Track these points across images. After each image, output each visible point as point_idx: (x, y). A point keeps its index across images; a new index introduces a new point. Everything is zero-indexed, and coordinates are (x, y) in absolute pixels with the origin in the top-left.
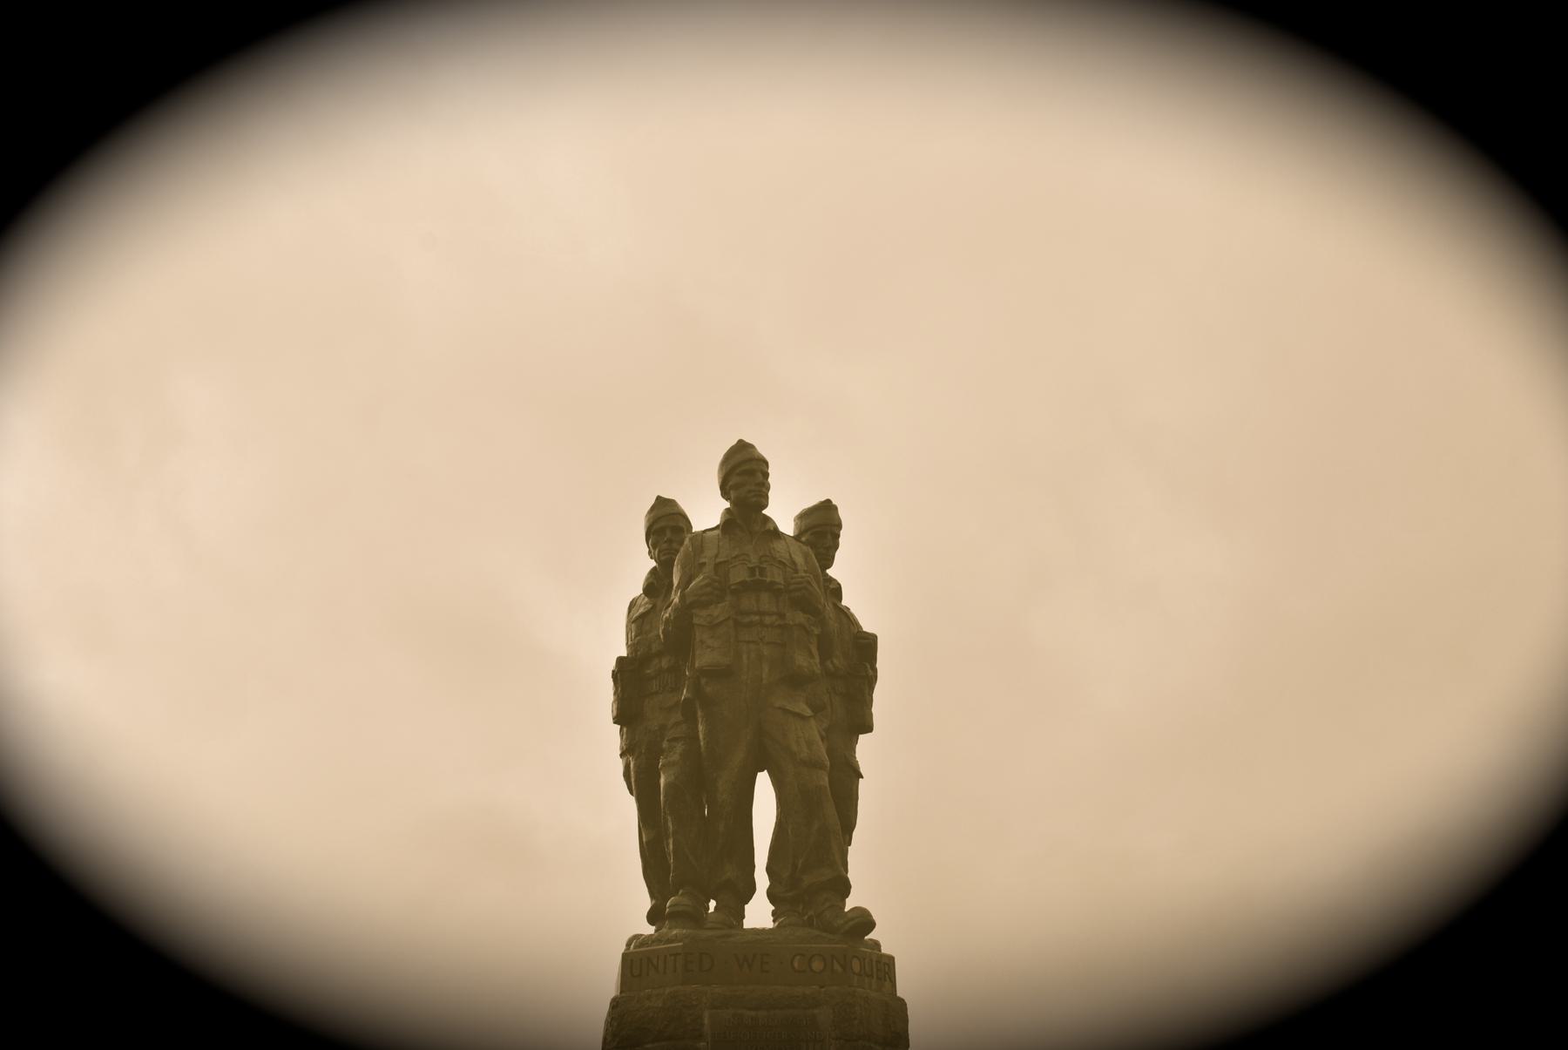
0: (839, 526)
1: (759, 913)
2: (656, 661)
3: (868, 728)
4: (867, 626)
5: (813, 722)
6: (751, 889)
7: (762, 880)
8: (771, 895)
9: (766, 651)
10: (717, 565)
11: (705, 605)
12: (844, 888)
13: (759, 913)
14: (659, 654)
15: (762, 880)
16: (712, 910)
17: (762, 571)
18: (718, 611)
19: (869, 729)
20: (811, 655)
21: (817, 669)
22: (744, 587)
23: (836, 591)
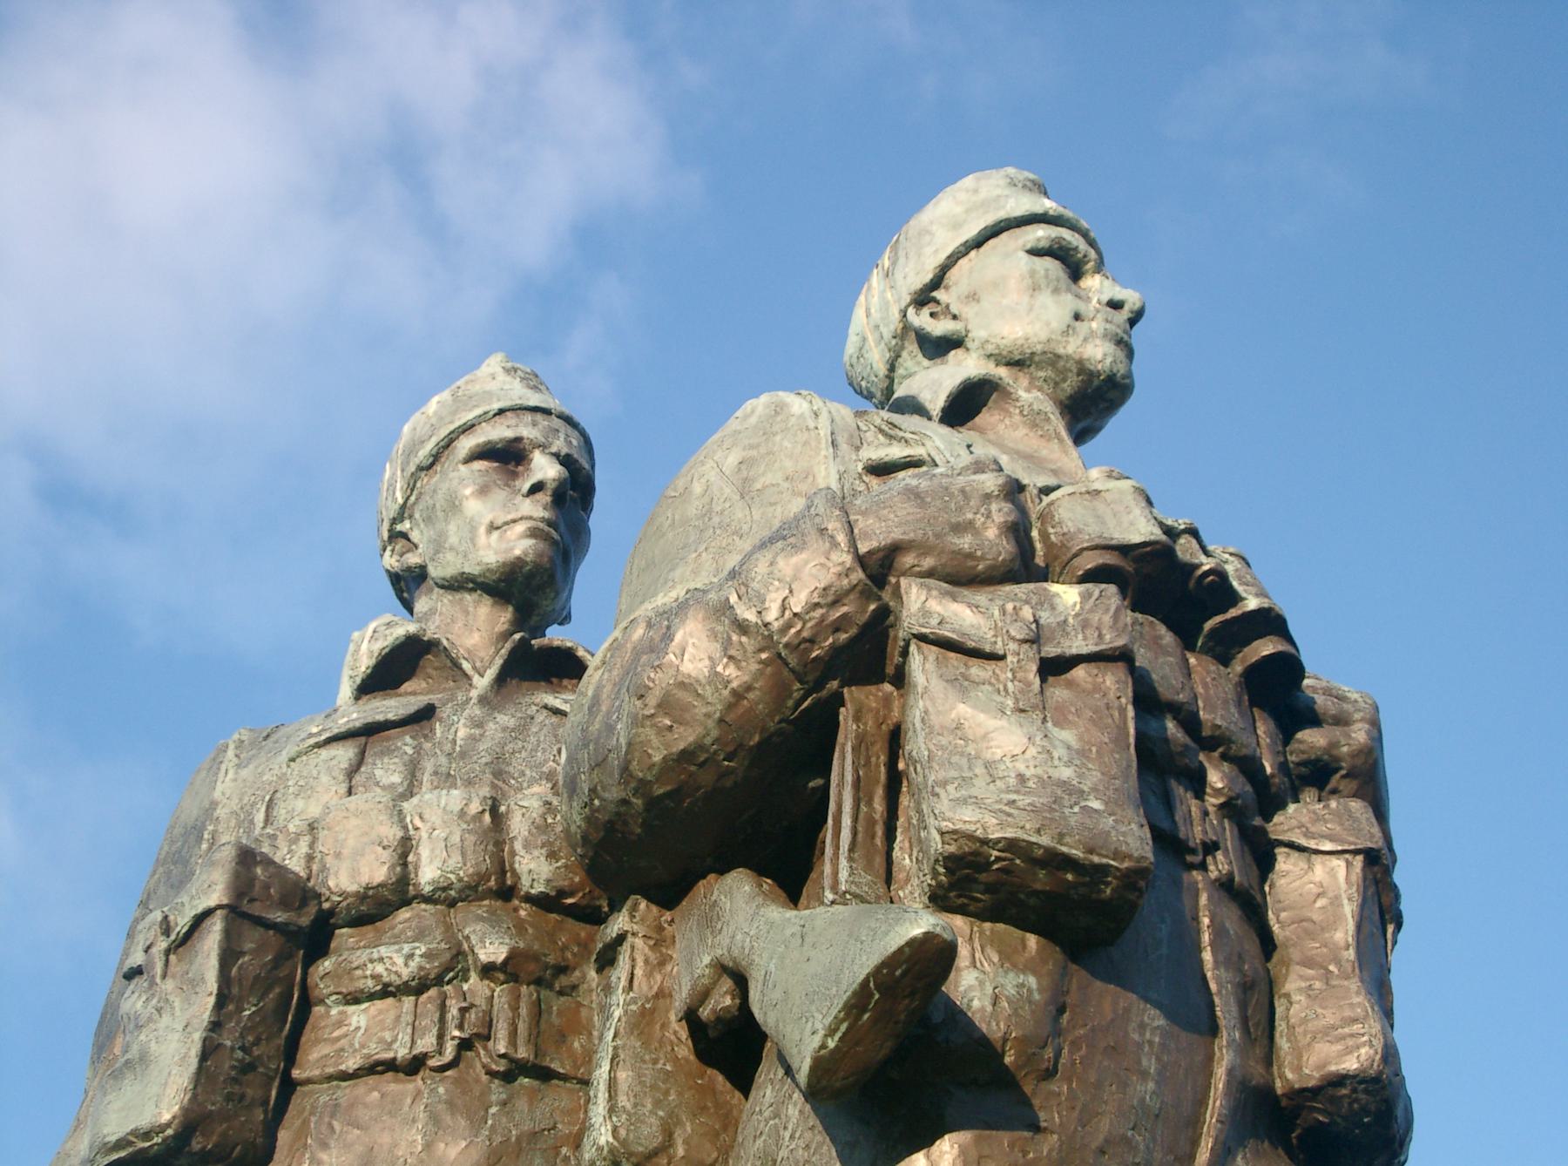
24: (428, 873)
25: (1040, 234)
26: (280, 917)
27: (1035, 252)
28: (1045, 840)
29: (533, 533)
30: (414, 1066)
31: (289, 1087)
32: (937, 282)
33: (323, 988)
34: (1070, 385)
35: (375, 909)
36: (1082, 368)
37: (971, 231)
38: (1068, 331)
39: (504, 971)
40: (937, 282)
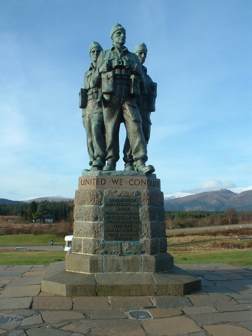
0: (147, 51)
1: (121, 165)
2: (91, 90)
3: (154, 110)
4: (154, 81)
5: (137, 108)
6: (117, 158)
7: (121, 155)
8: (125, 159)
9: (124, 87)
10: (109, 61)
11: (105, 72)
12: (144, 159)
13: (121, 165)
14: (93, 88)
15: (121, 155)
16: (106, 164)
17: (123, 62)
18: (110, 74)
19: (154, 110)
20: (138, 88)
21: (139, 93)
22: (117, 67)
23: (145, 70)
24: (91, 87)
25: (117, 32)
26: (84, 92)
27: (117, 33)
28: (106, 92)
29: (96, 58)
30: (92, 99)
31: (87, 101)
32: (112, 37)
33: (88, 95)
34: (120, 44)
35: (90, 89)
36: (120, 43)
37: (113, 33)
38: (119, 40)
39: (95, 92)
40: (112, 37)
